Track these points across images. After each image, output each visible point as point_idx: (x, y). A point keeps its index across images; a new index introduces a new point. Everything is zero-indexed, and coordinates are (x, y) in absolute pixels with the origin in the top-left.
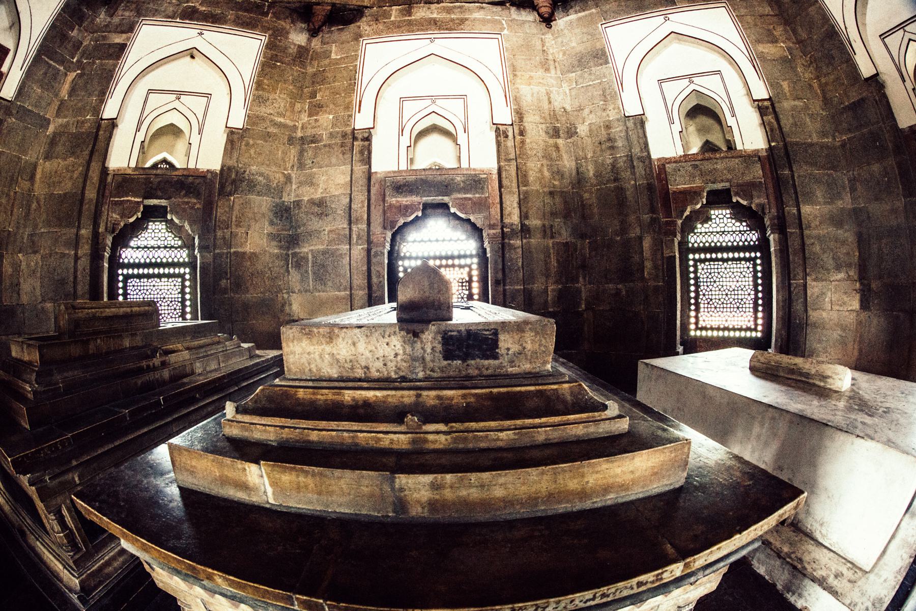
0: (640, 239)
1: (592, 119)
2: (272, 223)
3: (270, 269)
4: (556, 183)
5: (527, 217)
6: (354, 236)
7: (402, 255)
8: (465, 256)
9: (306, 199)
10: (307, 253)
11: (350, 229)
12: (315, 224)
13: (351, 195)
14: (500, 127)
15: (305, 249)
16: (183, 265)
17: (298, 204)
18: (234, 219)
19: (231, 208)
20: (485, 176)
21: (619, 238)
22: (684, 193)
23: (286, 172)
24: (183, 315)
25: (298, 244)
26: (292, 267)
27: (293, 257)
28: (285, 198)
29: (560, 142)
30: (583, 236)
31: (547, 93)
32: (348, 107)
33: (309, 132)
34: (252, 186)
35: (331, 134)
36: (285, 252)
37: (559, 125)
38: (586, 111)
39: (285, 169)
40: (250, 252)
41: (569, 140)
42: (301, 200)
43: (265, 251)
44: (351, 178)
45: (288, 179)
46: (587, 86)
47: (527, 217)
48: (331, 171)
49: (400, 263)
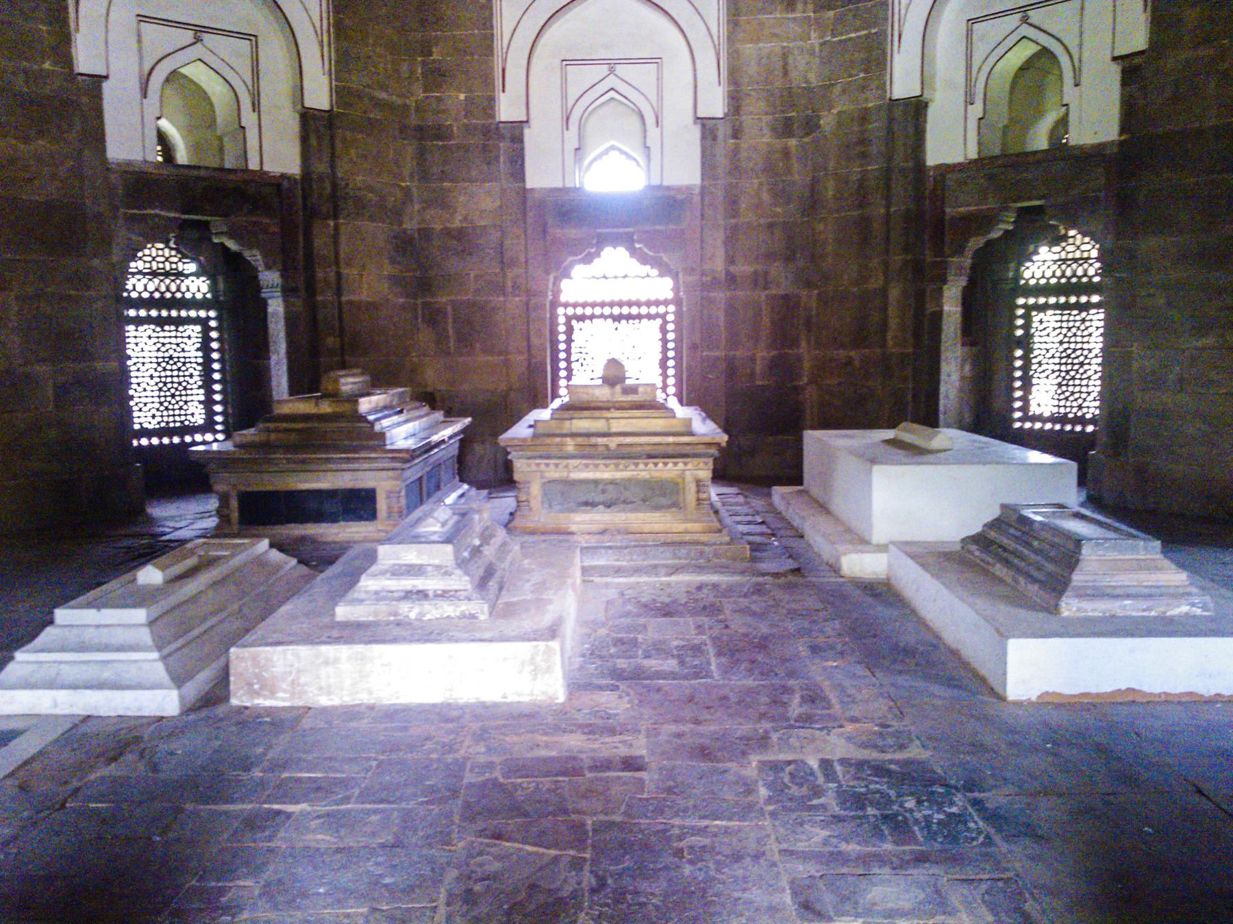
0: (884, 292)
1: (843, 105)
2: (393, 262)
8: (657, 303)
9: (438, 227)
14: (705, 121)
17: (426, 233)
22: (968, 219)
23: (403, 184)
26: (423, 320)
29: (793, 142)
30: (809, 284)
31: (784, 54)
32: (488, 81)
33: (430, 120)
34: (360, 204)
35: (466, 126)
37: (794, 114)
38: (837, 90)
41: (806, 140)
45: (407, 192)
46: (845, 41)
48: (473, 188)
49: (561, 311)
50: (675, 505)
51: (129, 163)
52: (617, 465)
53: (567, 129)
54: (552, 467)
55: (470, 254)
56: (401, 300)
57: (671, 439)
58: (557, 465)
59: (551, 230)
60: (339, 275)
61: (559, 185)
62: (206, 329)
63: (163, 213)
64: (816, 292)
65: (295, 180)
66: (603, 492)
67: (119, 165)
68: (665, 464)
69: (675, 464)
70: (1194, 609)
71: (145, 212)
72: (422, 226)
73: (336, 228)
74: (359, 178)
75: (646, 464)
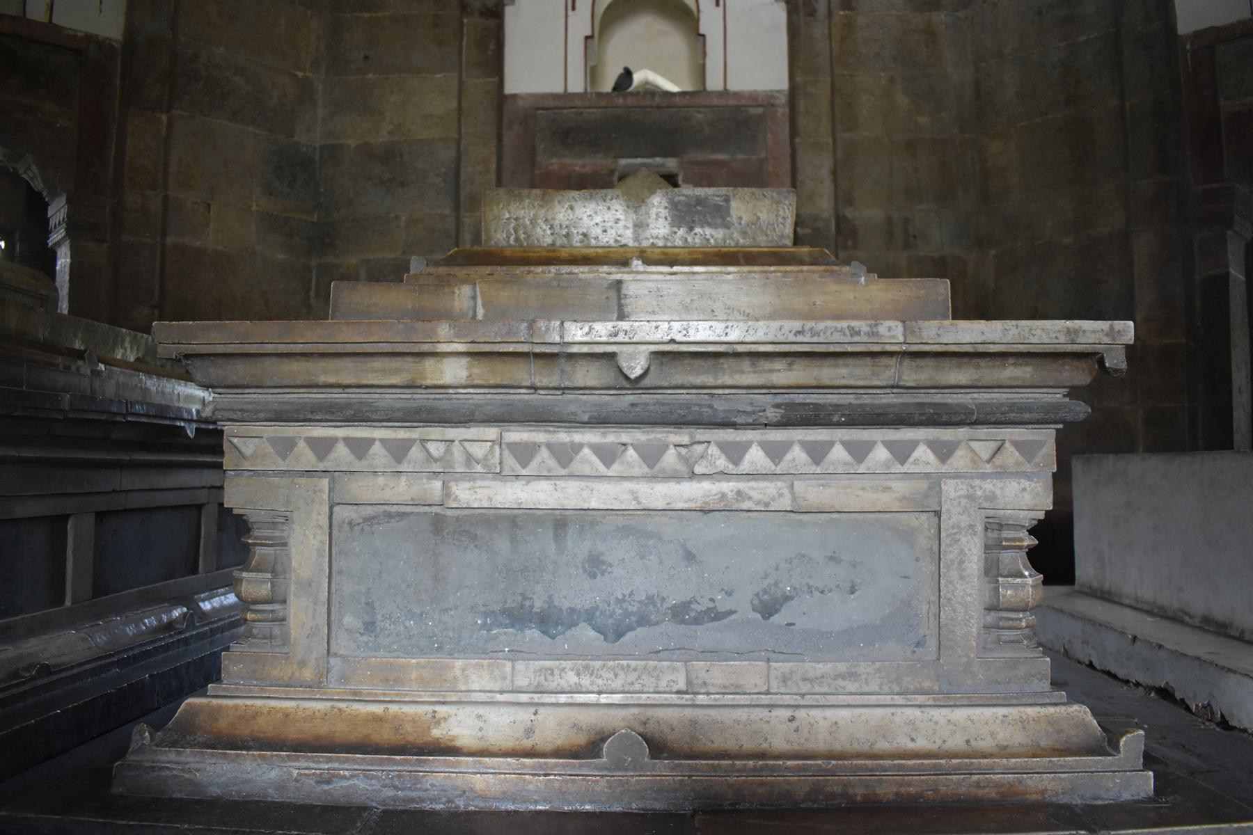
4: (922, 120)
5: (850, 202)
9: (352, 143)
13: (459, 142)
17: (332, 152)
20: (759, 111)
21: (1068, 241)
23: (300, 74)
28: (300, 137)
41: (961, 14)
44: (460, 103)
47: (850, 202)
52: (651, 456)
53: (574, 8)
55: (402, 185)
56: (280, 256)
58: (399, 451)
59: (540, 158)
60: (166, 199)
61: (559, 89)
64: (993, 252)
69: (901, 452)
72: (330, 142)
73: (170, 125)
75: (776, 452)
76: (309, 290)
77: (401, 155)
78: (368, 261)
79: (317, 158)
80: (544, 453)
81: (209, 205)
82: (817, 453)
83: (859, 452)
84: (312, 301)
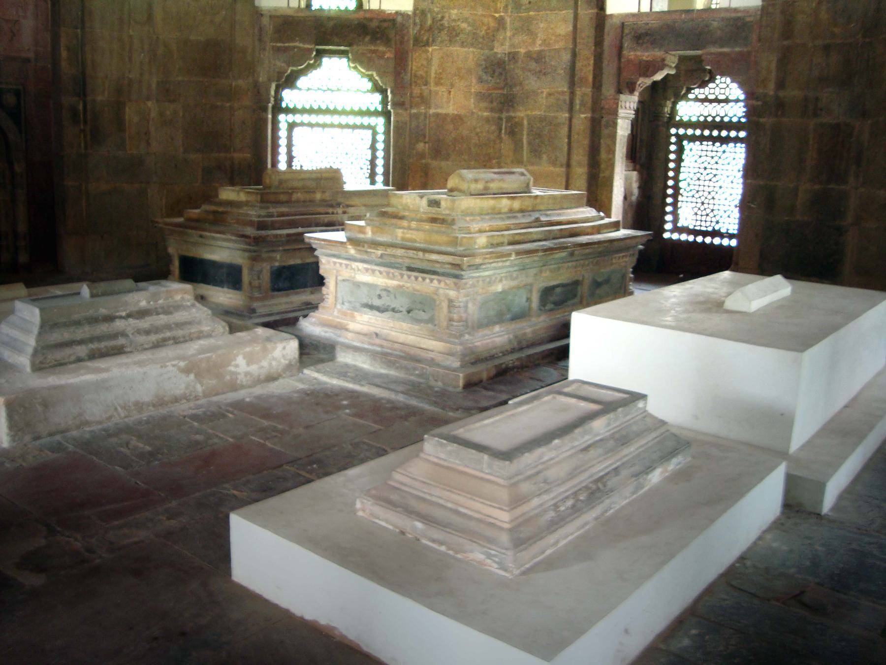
2: (480, 80)
3: (477, 134)
6: (577, 101)
7: (678, 118)
9: (522, 51)
10: (522, 119)
11: (572, 93)
12: (532, 83)
15: (521, 114)
16: (376, 113)
17: (513, 56)
18: (433, 75)
19: (429, 61)
23: (497, 15)
24: (372, 176)
25: (513, 106)
27: (507, 122)
36: (496, 115)
39: (496, 12)
40: (453, 114)
42: (518, 52)
43: (473, 113)
45: (501, 22)
49: (673, 131)
50: (431, 320)
51: (276, 9)
52: (388, 273)
54: (343, 265)
55: (545, 74)
56: (485, 114)
57: (421, 254)
59: (625, 52)
61: (635, 10)
62: (375, 134)
63: (301, 45)
65: (408, 15)
66: (380, 297)
67: (269, 11)
68: (424, 279)
69: (432, 280)
70: (489, 561)
71: (286, 45)
72: (513, 50)
74: (455, 12)
75: (409, 277)
76: (500, 130)
77: (545, 57)
78: (528, 116)
79: (506, 59)
80: (370, 271)
81: (450, 92)
82: (416, 278)
83: (424, 279)
84: (503, 135)
